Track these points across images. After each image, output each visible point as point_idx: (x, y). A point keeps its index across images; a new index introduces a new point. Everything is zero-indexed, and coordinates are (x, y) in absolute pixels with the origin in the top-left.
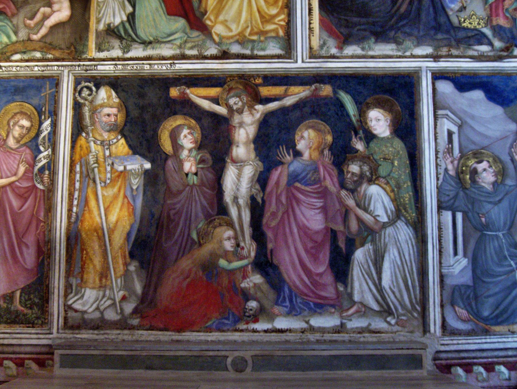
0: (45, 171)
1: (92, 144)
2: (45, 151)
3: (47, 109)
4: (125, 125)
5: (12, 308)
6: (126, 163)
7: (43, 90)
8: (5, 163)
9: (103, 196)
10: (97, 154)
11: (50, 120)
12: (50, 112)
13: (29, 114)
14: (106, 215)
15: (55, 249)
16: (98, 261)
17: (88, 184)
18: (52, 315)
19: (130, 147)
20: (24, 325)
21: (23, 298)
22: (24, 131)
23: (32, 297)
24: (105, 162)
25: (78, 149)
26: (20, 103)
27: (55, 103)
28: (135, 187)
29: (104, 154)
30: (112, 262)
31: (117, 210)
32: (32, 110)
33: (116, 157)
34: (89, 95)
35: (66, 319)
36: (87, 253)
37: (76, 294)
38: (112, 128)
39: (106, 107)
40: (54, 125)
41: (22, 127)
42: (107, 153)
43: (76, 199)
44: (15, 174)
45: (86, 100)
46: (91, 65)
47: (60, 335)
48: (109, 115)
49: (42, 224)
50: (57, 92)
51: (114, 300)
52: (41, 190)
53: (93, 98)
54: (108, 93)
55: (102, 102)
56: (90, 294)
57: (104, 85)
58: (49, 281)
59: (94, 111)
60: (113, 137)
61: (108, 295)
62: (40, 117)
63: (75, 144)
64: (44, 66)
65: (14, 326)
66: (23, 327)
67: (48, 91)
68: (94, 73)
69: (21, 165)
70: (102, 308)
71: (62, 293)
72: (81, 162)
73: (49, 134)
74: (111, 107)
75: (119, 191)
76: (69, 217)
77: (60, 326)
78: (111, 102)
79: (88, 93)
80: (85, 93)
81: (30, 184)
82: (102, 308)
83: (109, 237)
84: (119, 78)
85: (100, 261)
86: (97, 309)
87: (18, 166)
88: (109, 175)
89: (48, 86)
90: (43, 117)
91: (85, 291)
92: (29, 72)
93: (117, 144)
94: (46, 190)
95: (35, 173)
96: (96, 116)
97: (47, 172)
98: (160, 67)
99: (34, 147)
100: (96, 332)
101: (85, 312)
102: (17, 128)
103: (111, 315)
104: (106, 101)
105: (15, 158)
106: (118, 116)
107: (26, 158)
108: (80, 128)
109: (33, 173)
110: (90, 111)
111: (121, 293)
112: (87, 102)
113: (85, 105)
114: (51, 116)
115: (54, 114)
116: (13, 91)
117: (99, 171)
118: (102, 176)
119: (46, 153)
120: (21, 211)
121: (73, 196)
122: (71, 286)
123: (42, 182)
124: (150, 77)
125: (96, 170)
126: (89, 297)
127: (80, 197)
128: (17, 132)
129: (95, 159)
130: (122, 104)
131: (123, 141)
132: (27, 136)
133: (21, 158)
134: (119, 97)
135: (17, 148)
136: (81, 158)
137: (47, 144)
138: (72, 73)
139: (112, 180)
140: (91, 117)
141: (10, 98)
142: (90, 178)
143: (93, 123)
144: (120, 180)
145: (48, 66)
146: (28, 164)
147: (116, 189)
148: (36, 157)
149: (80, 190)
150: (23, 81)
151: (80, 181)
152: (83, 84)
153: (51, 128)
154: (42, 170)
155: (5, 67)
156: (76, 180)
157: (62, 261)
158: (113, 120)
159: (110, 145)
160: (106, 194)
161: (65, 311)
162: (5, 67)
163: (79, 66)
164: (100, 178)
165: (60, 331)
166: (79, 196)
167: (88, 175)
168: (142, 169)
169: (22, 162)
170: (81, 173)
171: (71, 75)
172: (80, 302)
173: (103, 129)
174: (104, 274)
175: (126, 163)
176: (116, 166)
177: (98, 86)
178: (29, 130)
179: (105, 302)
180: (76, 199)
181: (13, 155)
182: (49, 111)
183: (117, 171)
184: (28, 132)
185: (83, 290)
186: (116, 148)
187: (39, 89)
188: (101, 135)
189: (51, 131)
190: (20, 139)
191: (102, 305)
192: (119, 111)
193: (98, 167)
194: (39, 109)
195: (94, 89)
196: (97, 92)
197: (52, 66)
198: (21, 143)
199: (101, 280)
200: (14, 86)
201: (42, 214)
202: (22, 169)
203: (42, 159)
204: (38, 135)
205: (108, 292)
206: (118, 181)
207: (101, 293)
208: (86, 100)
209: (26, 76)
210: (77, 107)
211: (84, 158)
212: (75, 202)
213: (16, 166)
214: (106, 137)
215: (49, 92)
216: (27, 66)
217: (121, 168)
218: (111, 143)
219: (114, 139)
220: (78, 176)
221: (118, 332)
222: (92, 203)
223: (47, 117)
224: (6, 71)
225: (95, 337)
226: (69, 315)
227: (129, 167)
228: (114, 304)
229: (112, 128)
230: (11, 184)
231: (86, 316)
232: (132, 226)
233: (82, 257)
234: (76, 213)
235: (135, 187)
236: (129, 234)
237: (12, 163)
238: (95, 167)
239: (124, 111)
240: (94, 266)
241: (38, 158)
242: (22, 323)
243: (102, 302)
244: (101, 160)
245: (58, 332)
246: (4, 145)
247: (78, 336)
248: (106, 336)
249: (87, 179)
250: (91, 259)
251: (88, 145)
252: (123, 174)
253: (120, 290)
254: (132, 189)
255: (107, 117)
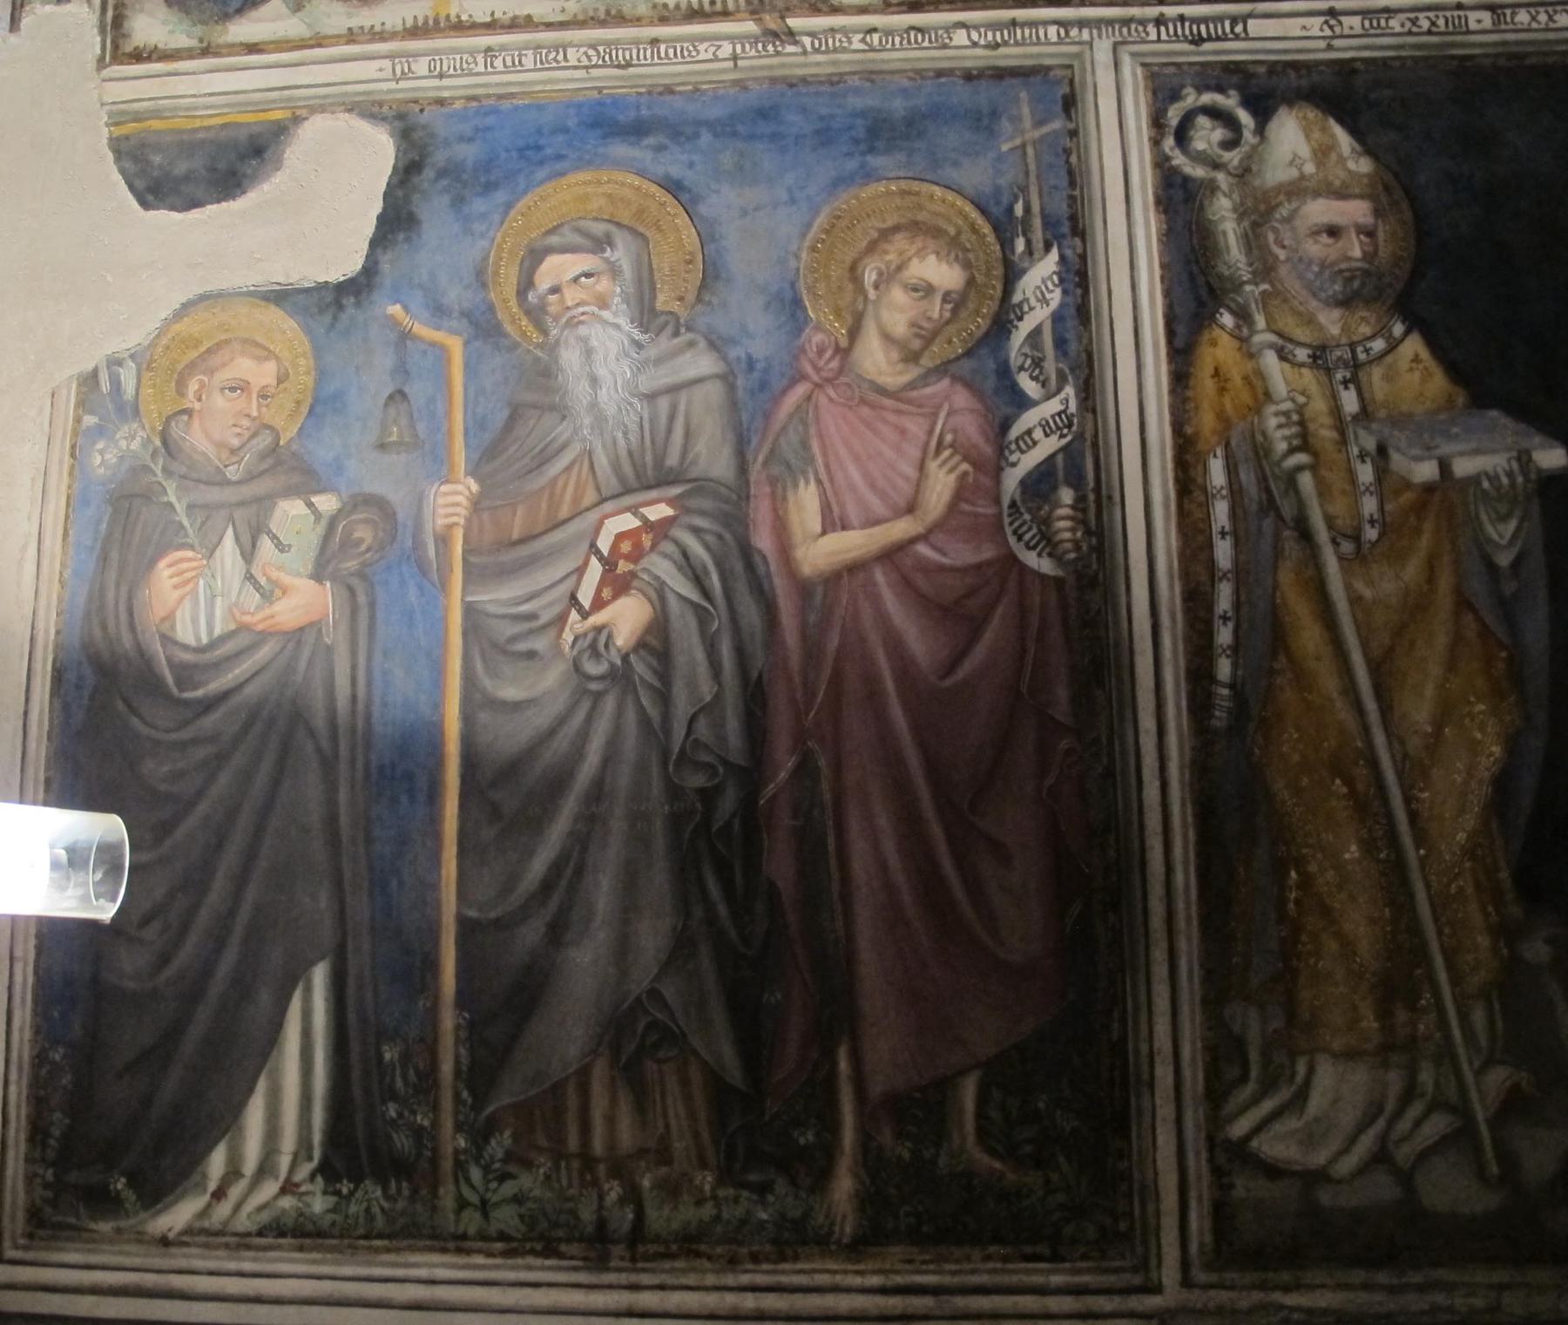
0: (1055, 488)
1: (1270, 360)
2: (1048, 397)
3: (1036, 208)
4: (1416, 274)
5: (942, 1161)
6: (1446, 448)
7: (1005, 125)
8: (857, 458)
9: (1355, 600)
10: (1300, 409)
11: (1054, 255)
12: (1048, 223)
13: (952, 231)
14: (1379, 690)
15: (1143, 864)
16: (1360, 920)
17: (1278, 552)
18: (1150, 1192)
19: (1454, 371)
20: (1009, 1250)
21: (994, 1114)
22: (936, 309)
23: (1041, 1105)
24: (1343, 441)
25: (1205, 384)
26: (903, 184)
27: (1072, 184)
28: (1504, 560)
29: (1336, 410)
30: (1436, 920)
31: (1435, 670)
32: (961, 212)
33: (1399, 420)
34: (1229, 145)
35: (1221, 1212)
36: (1306, 883)
37: (1268, 1086)
38: (1356, 291)
39: (1317, 194)
40: (1079, 278)
41: (927, 290)
42: (1350, 401)
43: (1225, 618)
44: (911, 509)
45: (1216, 166)
46: (1219, 19)
47: (1196, 1298)
48: (1333, 231)
49: (1064, 744)
50: (1073, 134)
51: (1462, 1110)
52: (1043, 577)
53: (1249, 156)
54: (1316, 135)
55: (1295, 173)
56: (1336, 1087)
57: (1290, 104)
58: (1123, 1020)
59: (1259, 213)
60: (1365, 330)
61: (1430, 1088)
62: (1006, 244)
63: (1190, 364)
64: (995, 26)
65: (958, 1252)
66: (1005, 1259)
67: (1025, 127)
68: (1235, 51)
69: (932, 466)
70: (1404, 1154)
71: (1194, 1078)
72: (1227, 445)
73: (1057, 318)
74: (1341, 194)
75: (1431, 580)
76: (1200, 704)
77: (1194, 1248)
78: (1337, 177)
79: (1219, 134)
80: (1207, 135)
81: (988, 553)
82: (1404, 1154)
83: (1408, 800)
84: (1354, 71)
85: (1373, 921)
86: (1381, 1157)
87: (922, 467)
88: (1369, 505)
89: (1026, 110)
90: (1020, 245)
91: (1311, 1070)
92: (926, 55)
93: (1389, 359)
94: (1071, 580)
95: (1006, 502)
96: (1271, 237)
97: (1066, 495)
98: (1543, 18)
99: (991, 383)
100: (1382, 1277)
101: (1320, 1176)
102: (898, 295)
103: (1451, 1190)
104: (1310, 168)
105: (903, 432)
106: (1381, 235)
107: (955, 431)
108: (1203, 292)
109: (997, 501)
110: (1241, 213)
111: (1498, 1077)
112: (1221, 177)
113: (1212, 187)
114: (1059, 238)
115: (1072, 228)
116: (860, 132)
117: (1323, 490)
118: (1339, 507)
119: (1054, 406)
120: (948, 682)
121: (1210, 607)
122: (1239, 1044)
123: (1047, 541)
124: (1502, 62)
125: (1306, 481)
126: (1335, 1101)
127: (1245, 610)
128: (897, 312)
129: (1294, 430)
130: (1389, 177)
131: (1414, 345)
132: (952, 329)
133: (931, 432)
134: (1370, 151)
135: (911, 386)
136: (1225, 422)
137: (1050, 366)
138: (1133, 55)
139: (1384, 524)
140: (1253, 240)
141: (851, 165)
142: (1280, 517)
143: (1265, 269)
144: (1428, 527)
145: (1014, 23)
146: (966, 458)
147: (1412, 571)
148: (1005, 427)
149: (1240, 574)
150: (904, 92)
151: (1235, 534)
152: (1191, 99)
153: (1065, 292)
154: (1040, 484)
155: (812, 34)
156: (1215, 529)
157: (1181, 924)
158: (1357, 253)
159: (1356, 366)
160: (1367, 593)
161: (1217, 1171)
162: (812, 34)
163: (1160, 21)
164: (1330, 521)
165: (1201, 1276)
166: (1237, 605)
167: (1269, 505)
168: (1525, 470)
169: (938, 452)
170: (1235, 491)
171: (1126, 60)
172: (1292, 1123)
173: (1314, 295)
174: (1399, 980)
175: (1446, 448)
176: (1397, 461)
177: (1263, 108)
178: (956, 302)
179: (1418, 1124)
180: (1225, 618)
181: (892, 418)
182: (1044, 216)
183: (1407, 485)
184: (955, 311)
185: (1301, 1069)
186: (1388, 378)
187: (984, 122)
188: (1310, 321)
189: (1062, 305)
190: (916, 344)
191: (1403, 1139)
192: (1377, 213)
193: (1313, 468)
194: (995, 210)
195: (1245, 117)
196: (1260, 130)
197: (1033, 24)
198: (926, 362)
199: (1384, 1014)
200: (862, 114)
201: (1062, 693)
202: (941, 485)
203: (1038, 434)
204: (1002, 325)
205: (1426, 1077)
206: (1418, 531)
207: (1395, 1080)
208: (1216, 166)
209: (919, 72)
210: (1179, 199)
211: (1239, 428)
212: (1224, 636)
213: (911, 472)
214: (1335, 330)
215: (1037, 134)
216: (919, 30)
217: (1426, 471)
218: (1362, 357)
219: (1372, 337)
220: (1221, 512)
221: (1499, 1276)
222: (1309, 637)
223: (1039, 244)
224: (817, 51)
225: (1377, 1301)
226: (1239, 1192)
227: (1463, 467)
228: (1462, 1136)
229: (1356, 291)
230: (891, 555)
231: (1325, 1197)
232: (1513, 744)
233: (1282, 902)
234: (1232, 686)
235: (1504, 560)
236: (1503, 783)
237: (889, 453)
238: (1300, 468)
239: (1408, 215)
240: (1348, 947)
241: (1015, 432)
242: (998, 1239)
243: (1404, 1125)
244: (1325, 433)
245: (1186, 1282)
246: (841, 371)
247: (1292, 1300)
248: (1440, 1298)
249: (1268, 524)
250: (1326, 911)
251: (1250, 365)
252: (1437, 497)
253: (1489, 1063)
254: (1491, 567)
255: (1325, 239)
